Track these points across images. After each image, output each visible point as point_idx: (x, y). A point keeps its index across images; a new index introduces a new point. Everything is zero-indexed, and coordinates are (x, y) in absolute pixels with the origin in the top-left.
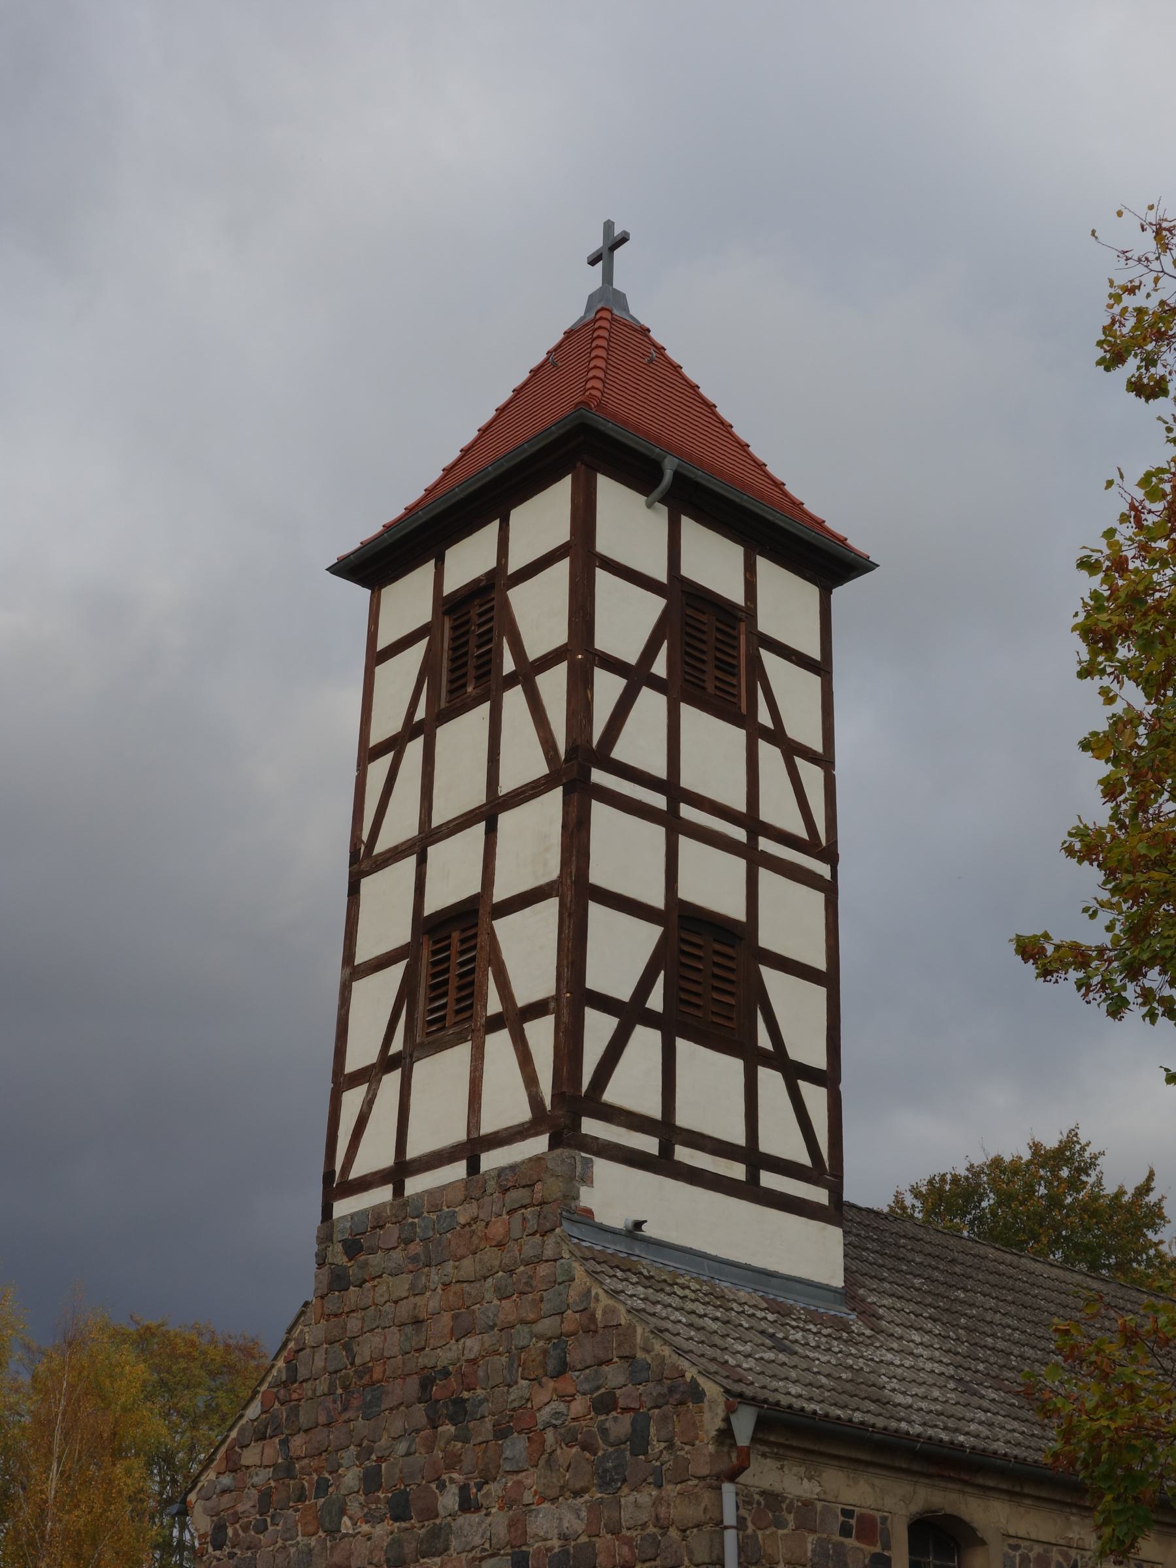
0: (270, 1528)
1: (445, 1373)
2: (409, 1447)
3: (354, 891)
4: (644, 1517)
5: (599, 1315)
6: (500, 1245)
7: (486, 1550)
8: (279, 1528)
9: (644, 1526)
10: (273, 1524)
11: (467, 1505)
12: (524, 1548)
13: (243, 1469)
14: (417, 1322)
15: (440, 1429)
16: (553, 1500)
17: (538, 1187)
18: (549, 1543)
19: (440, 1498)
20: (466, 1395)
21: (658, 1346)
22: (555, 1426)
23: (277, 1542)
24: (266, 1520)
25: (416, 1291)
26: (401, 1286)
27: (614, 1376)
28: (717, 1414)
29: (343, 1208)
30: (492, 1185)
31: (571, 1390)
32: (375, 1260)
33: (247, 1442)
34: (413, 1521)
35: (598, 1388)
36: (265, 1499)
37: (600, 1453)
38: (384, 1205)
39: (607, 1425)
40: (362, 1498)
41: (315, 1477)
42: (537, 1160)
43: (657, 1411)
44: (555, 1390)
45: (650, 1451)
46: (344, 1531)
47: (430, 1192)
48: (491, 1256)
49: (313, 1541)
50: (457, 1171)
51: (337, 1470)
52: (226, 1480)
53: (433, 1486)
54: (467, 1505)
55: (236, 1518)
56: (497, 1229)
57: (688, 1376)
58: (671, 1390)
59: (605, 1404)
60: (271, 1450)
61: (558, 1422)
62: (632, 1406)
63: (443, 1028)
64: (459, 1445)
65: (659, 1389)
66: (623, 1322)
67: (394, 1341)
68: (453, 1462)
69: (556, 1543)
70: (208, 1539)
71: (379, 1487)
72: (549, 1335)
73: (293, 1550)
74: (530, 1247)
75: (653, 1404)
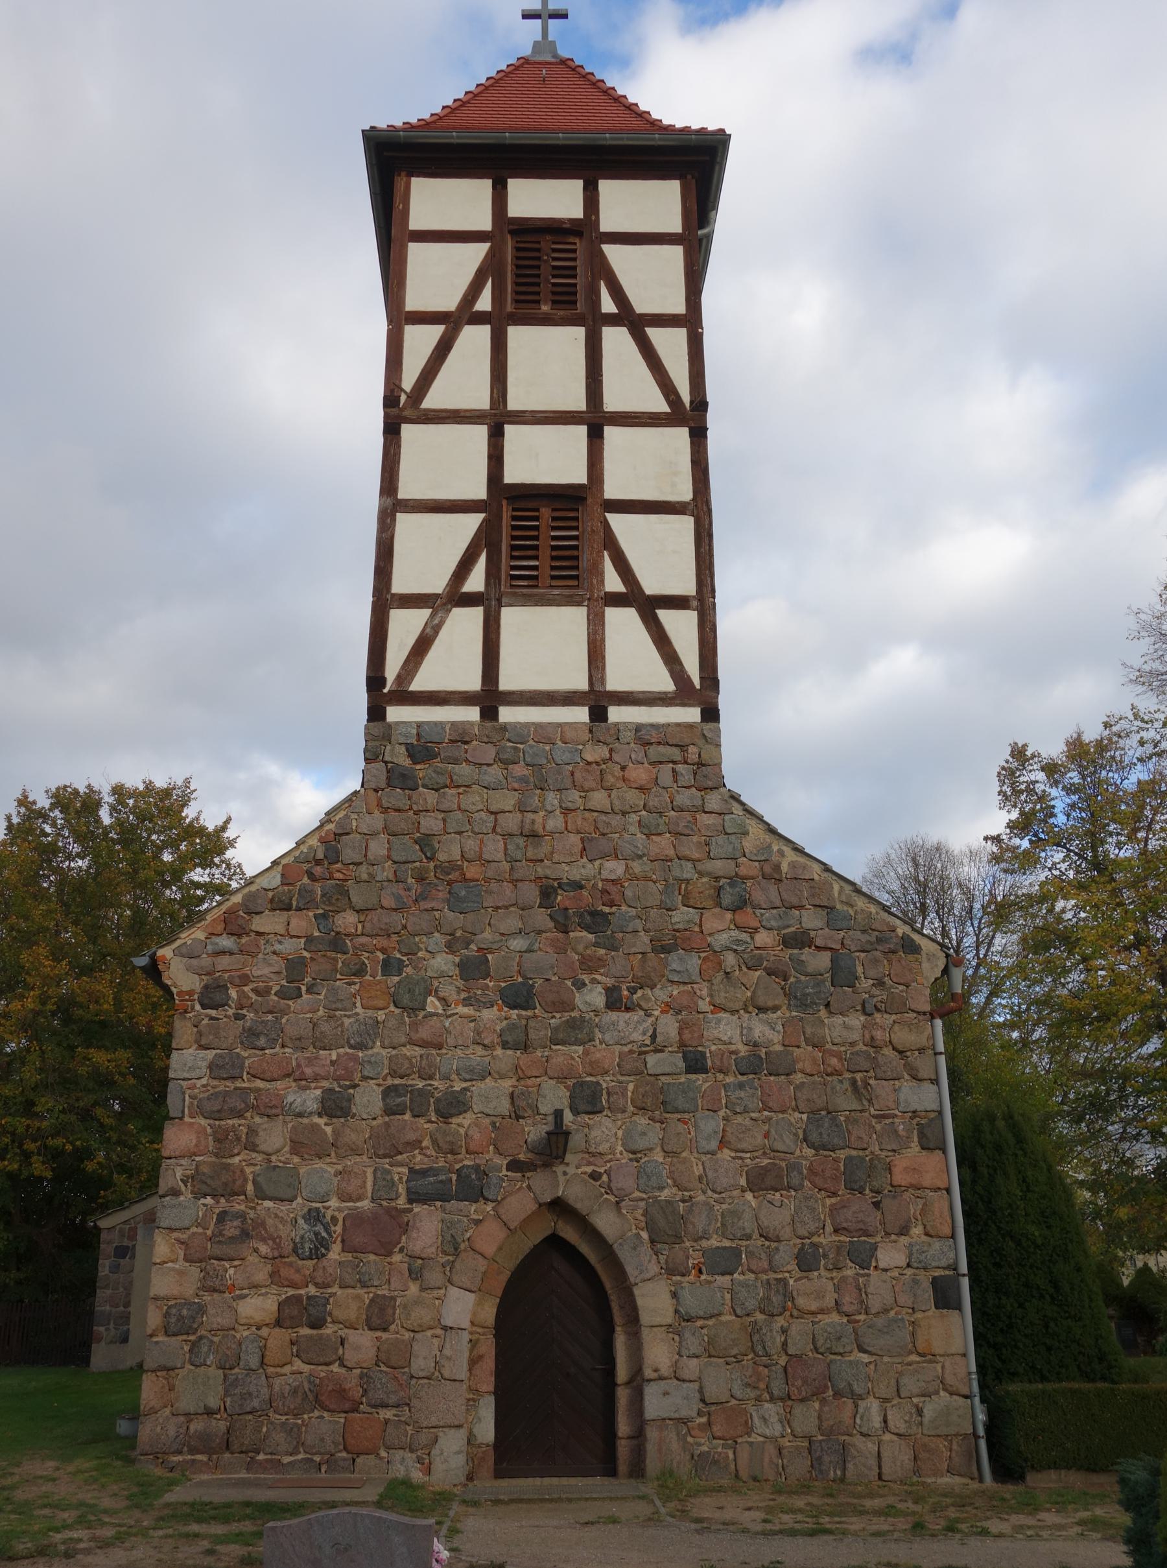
0: (305, 996)
1: (577, 886)
2: (531, 944)
3: (392, 431)
4: (856, 1036)
5: (785, 867)
6: (641, 789)
7: (648, 1046)
8: (322, 997)
9: (852, 1044)
10: (309, 991)
11: (614, 1002)
12: (700, 1049)
13: (252, 934)
14: (533, 836)
15: (572, 934)
16: (734, 1012)
17: (691, 749)
18: (733, 1048)
19: (577, 995)
20: (606, 910)
21: (861, 903)
22: (735, 951)
23: (319, 1010)
24: (300, 988)
25: (522, 809)
26: (507, 800)
27: (811, 920)
28: (937, 965)
29: (395, 714)
30: (628, 736)
31: (756, 924)
32: (464, 771)
33: (259, 909)
34: (536, 1011)
35: (788, 927)
36: (295, 968)
37: (792, 980)
38: (471, 724)
39: (803, 958)
40: (460, 983)
41: (381, 956)
42: (690, 726)
43: (863, 955)
44: (733, 921)
45: (858, 985)
46: (429, 1009)
47: (539, 726)
48: (633, 797)
49: (381, 1015)
50: (581, 714)
51: (416, 954)
52: (226, 942)
53: (569, 983)
54: (614, 1002)
55: (245, 979)
56: (640, 774)
57: (900, 932)
58: (879, 940)
59: (800, 940)
60: (301, 922)
61: (739, 948)
62: (833, 946)
63: (536, 586)
64: (602, 951)
65: (864, 938)
66: (816, 877)
67: (494, 848)
68: (590, 965)
69: (743, 1050)
70: (196, 997)
71: (487, 975)
72: (721, 874)
73: (347, 1021)
74: (685, 798)
75: (859, 948)
